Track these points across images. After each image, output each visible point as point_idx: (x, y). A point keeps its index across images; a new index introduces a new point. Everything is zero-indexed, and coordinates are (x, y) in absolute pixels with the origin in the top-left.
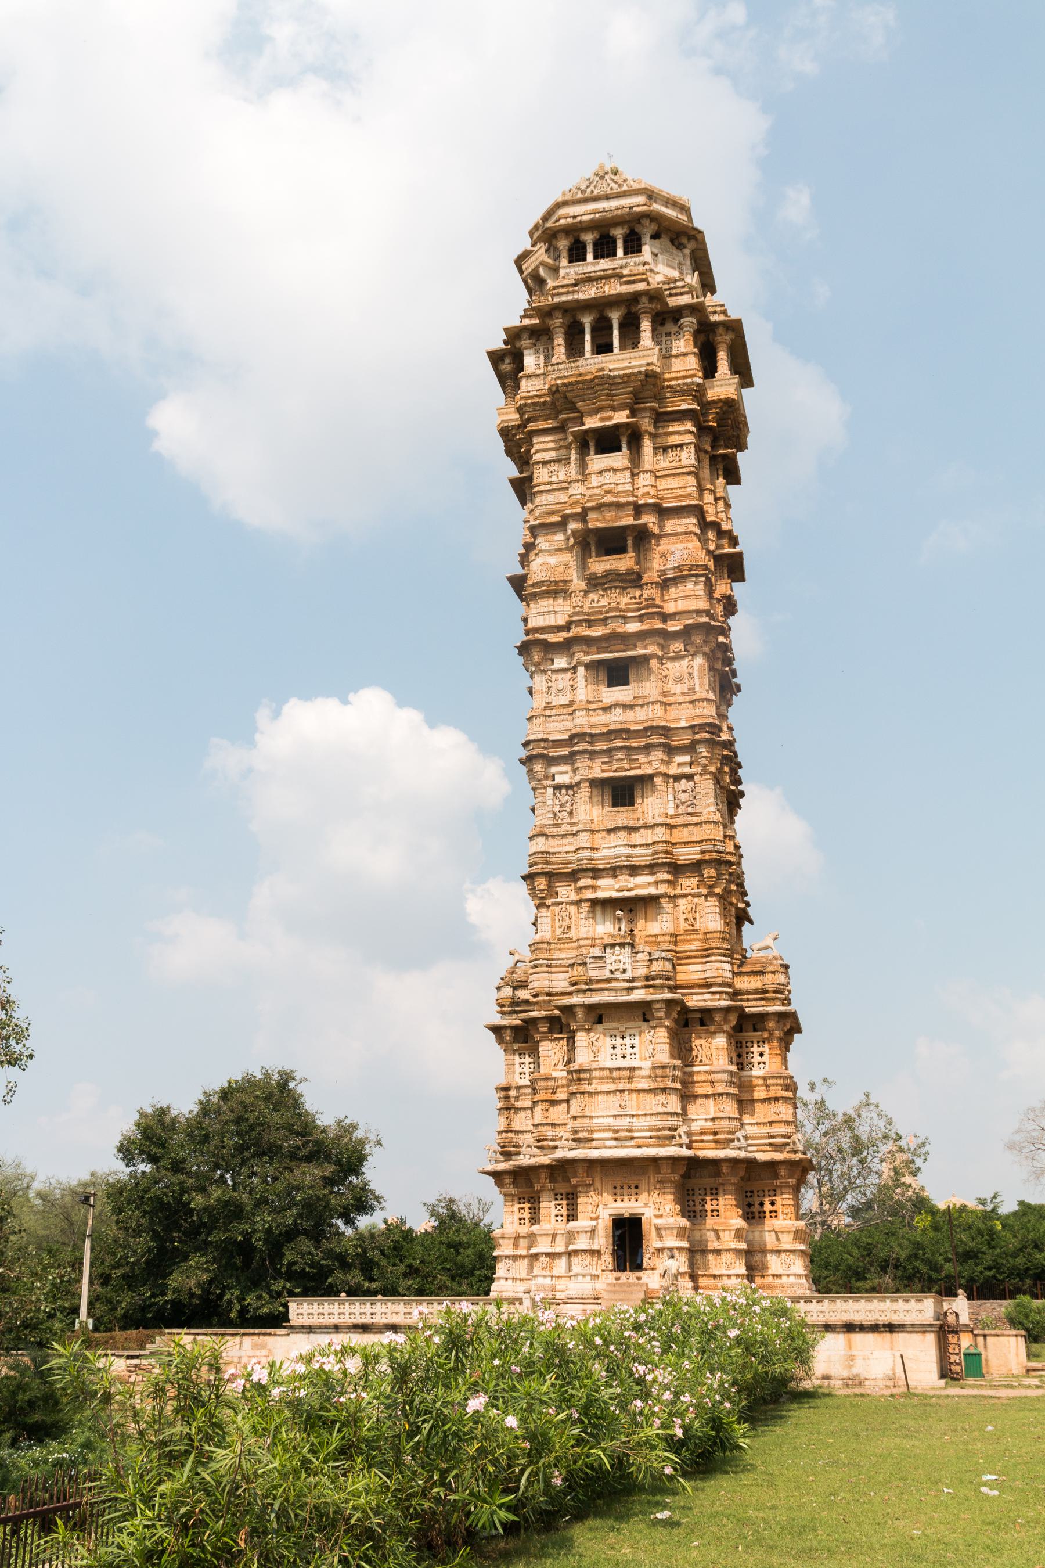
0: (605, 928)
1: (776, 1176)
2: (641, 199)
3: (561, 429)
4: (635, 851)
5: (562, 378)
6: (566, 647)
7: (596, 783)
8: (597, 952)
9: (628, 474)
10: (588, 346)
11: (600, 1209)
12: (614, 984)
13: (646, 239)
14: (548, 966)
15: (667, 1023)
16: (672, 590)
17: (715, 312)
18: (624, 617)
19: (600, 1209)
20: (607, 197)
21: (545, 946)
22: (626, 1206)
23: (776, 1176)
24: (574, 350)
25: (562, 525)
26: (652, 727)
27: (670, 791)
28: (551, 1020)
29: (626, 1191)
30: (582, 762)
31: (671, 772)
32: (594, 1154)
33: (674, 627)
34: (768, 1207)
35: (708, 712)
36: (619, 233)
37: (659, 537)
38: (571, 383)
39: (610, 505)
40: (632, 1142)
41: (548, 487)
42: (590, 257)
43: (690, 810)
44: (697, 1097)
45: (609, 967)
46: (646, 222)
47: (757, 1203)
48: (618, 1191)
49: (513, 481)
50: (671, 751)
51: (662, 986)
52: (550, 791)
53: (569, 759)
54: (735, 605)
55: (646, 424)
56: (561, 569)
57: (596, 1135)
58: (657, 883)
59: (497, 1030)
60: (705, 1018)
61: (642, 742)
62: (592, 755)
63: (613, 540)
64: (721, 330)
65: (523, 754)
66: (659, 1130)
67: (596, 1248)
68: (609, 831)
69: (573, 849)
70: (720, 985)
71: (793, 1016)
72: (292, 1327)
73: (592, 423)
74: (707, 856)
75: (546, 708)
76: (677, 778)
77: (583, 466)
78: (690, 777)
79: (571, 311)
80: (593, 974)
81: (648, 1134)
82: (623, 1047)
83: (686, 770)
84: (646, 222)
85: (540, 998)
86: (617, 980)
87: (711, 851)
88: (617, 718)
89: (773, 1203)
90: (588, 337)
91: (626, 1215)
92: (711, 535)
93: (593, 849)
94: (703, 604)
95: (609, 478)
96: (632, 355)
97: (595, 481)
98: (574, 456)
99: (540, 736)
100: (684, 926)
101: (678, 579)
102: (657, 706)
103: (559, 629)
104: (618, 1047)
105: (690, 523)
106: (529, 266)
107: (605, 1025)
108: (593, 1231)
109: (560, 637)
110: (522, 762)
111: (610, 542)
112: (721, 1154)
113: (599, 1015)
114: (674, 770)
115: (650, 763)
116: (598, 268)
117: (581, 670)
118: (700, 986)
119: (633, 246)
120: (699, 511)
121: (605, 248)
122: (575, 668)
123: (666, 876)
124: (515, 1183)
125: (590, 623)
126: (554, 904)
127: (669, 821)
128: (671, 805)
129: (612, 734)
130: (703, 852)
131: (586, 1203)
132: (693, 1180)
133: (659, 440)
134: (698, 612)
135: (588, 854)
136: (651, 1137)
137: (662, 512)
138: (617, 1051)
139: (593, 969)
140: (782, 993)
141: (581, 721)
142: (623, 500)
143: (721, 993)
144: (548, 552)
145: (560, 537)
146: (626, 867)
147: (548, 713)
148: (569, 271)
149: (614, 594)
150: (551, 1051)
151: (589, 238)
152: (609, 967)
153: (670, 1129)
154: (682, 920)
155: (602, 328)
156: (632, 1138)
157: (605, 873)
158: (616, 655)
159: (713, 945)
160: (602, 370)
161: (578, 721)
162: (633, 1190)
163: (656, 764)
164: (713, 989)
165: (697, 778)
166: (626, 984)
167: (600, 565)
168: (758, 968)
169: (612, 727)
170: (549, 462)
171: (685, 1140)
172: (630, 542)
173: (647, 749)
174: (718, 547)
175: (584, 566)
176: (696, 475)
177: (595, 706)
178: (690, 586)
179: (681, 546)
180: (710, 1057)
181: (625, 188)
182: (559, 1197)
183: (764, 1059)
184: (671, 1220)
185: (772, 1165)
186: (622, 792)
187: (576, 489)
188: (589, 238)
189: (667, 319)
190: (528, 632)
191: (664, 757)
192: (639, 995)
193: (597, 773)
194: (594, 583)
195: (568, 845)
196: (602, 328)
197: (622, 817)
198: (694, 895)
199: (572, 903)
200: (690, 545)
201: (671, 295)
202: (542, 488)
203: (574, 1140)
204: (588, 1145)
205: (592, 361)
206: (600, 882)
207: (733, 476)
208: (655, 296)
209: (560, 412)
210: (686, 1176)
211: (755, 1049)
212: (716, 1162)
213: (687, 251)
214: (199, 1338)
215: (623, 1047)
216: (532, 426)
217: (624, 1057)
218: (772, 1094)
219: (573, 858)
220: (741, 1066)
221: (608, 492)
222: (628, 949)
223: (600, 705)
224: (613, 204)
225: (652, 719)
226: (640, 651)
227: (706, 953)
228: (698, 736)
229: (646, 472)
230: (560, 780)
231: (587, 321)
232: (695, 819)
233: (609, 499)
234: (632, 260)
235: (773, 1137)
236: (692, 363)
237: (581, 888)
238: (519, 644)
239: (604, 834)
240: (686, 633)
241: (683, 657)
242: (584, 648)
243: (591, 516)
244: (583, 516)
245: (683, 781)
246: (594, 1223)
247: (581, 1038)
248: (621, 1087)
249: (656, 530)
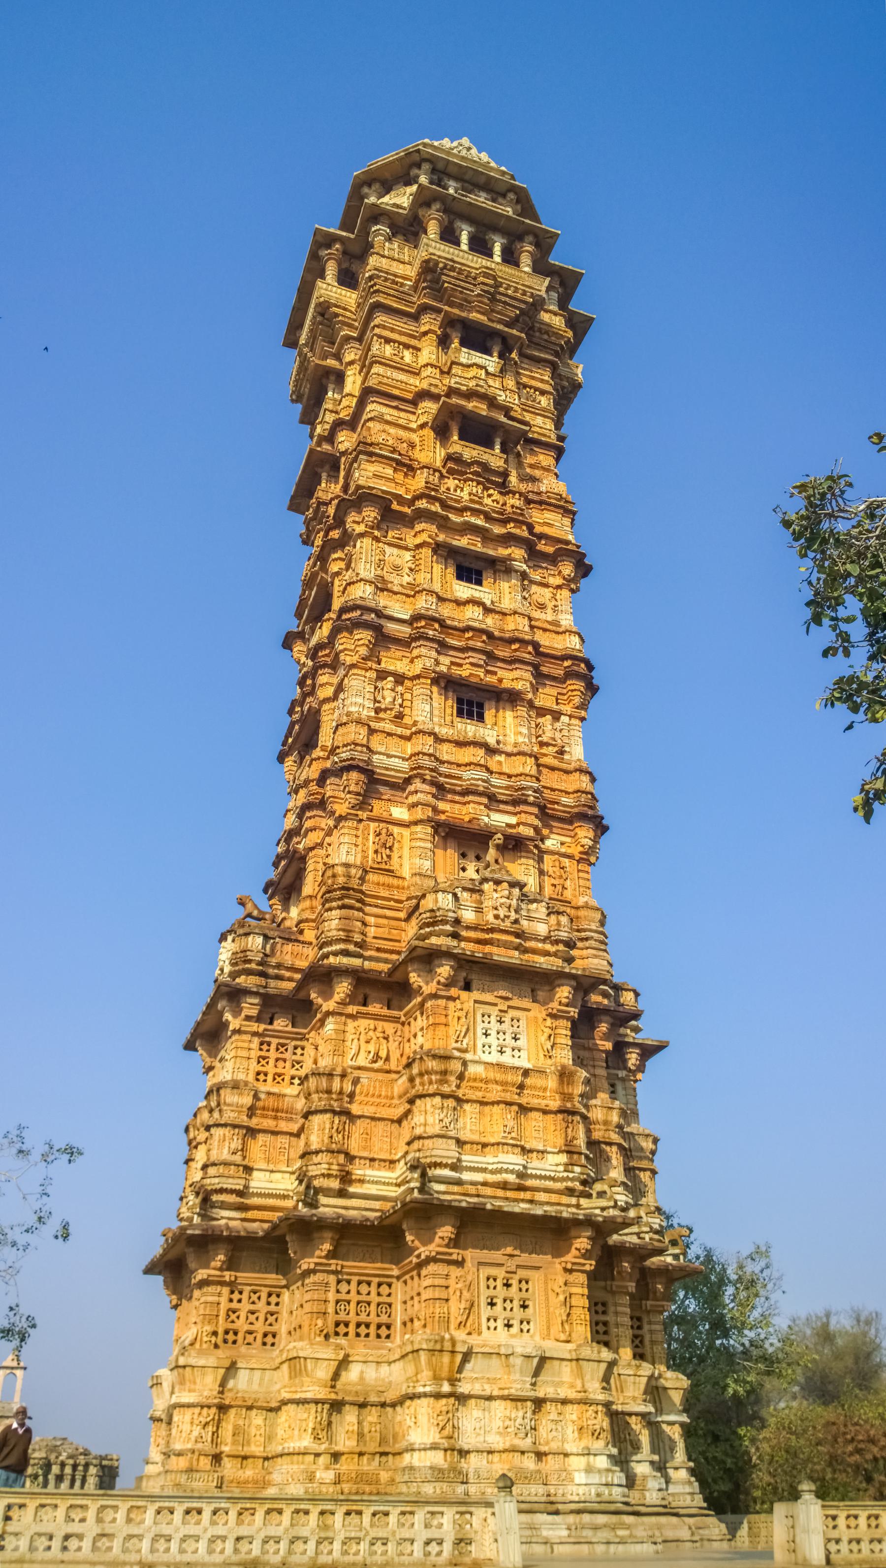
31: (537, 703)
76: (542, 712)
82: (501, 1036)
104: (493, 1033)
107: (476, 995)
117: (427, 552)
138: (492, 1039)
206: (442, 805)
215: (501, 1036)
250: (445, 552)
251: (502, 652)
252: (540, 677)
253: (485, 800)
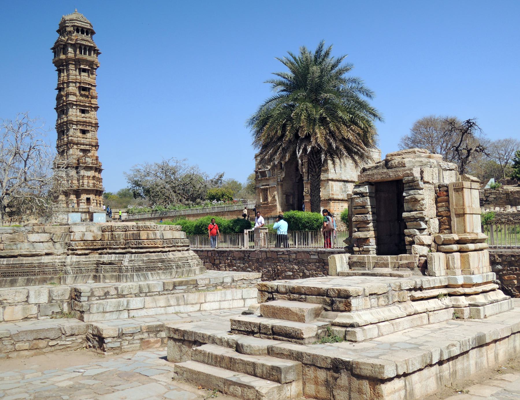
0: (81, 154)
6: (76, 105)
7: (80, 130)
22: (88, 196)
25: (75, 83)
30: (79, 126)
33: (93, 106)
50: (92, 127)
53: (77, 125)
62: (80, 125)
63: (84, 89)
73: (82, 67)
79: (81, 45)
88: (84, 119)
95: (85, 77)
97: (82, 77)
98: (78, 70)
109: (75, 103)
111: (84, 89)
115: (88, 128)
119: (87, 34)
121: (83, 33)
129: (83, 122)
141: (79, 119)
173: (89, 126)
175: (80, 92)
186: (84, 132)
192: (90, 165)
194: (81, 95)
195: (76, 139)
216: (70, 62)
244: (80, 83)
250: (80, 109)
251: (88, 124)
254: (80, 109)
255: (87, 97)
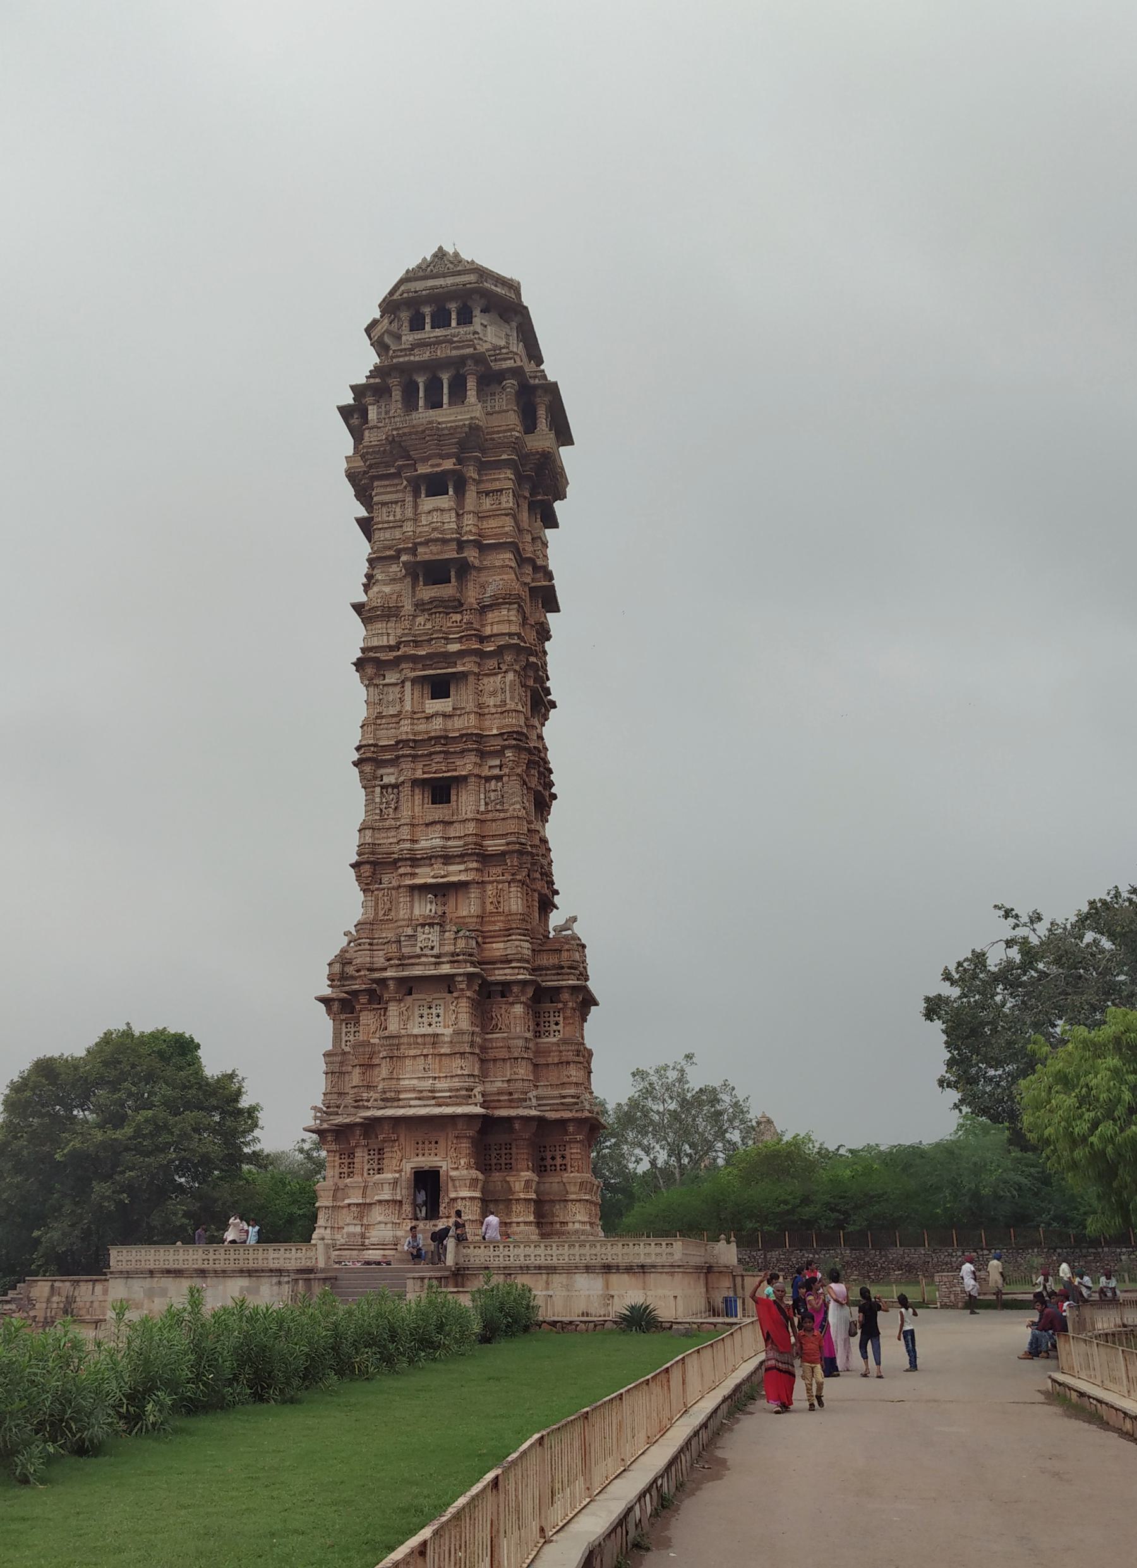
1: (566, 1133)
2: (472, 278)
3: (398, 475)
4: (450, 843)
5: (396, 429)
6: (396, 663)
7: (415, 783)
8: (409, 931)
9: (453, 514)
10: (421, 403)
11: (404, 1163)
12: (423, 959)
13: (477, 312)
14: (370, 944)
15: (468, 994)
16: (490, 615)
17: (535, 377)
18: (446, 639)
19: (404, 1163)
20: (444, 276)
21: (368, 926)
22: (426, 1161)
23: (566, 1133)
24: (410, 403)
26: (467, 734)
27: (482, 790)
28: (371, 992)
29: (427, 1145)
30: (406, 765)
32: (400, 1112)
34: (559, 1161)
35: (515, 722)
36: (453, 306)
37: (479, 569)
38: (405, 434)
39: (437, 540)
40: (433, 1102)
41: (386, 525)
42: (428, 327)
43: (498, 807)
44: (495, 1060)
45: (419, 945)
46: (476, 297)
47: (549, 1157)
48: (420, 1145)
49: (360, 521)
50: (483, 754)
51: (466, 961)
52: (378, 789)
54: (549, 632)
55: (471, 473)
56: (395, 596)
57: (402, 1096)
58: (466, 870)
59: (325, 1001)
60: (505, 988)
61: (459, 747)
64: (539, 392)
65: (356, 756)
66: (457, 1090)
67: (399, 1198)
68: (427, 825)
69: (395, 840)
70: (519, 961)
71: (585, 989)
72: (111, 1273)
73: (423, 469)
74: (511, 847)
75: (377, 718)
76: (488, 779)
77: (416, 506)
78: (499, 778)
79: (406, 372)
80: (406, 950)
81: (448, 1094)
83: (496, 772)
84: (476, 297)
85: (362, 973)
86: (426, 956)
87: (514, 843)
88: (437, 725)
89: (563, 1157)
90: (421, 394)
91: (426, 1168)
92: (528, 569)
93: (413, 841)
94: (514, 629)
95: (436, 517)
96: (459, 410)
98: (409, 499)
99: (371, 742)
100: (490, 908)
101: (494, 606)
102: (472, 716)
103: (391, 648)
104: (425, 1016)
105: (507, 557)
106: (376, 333)
107: (414, 996)
108: (396, 1182)
110: (355, 764)
111: (435, 572)
112: (513, 1113)
113: (408, 986)
114: (486, 772)
115: (466, 766)
116: (435, 334)
117: (408, 685)
118: (502, 962)
119: (465, 318)
120: (515, 548)
121: (442, 320)
122: (403, 682)
123: (475, 865)
124: (337, 1140)
125: (417, 644)
126: (377, 889)
127: (479, 817)
128: (483, 802)
130: (508, 844)
131: (392, 1159)
132: (490, 1138)
133: (482, 486)
134: (510, 635)
135: (408, 845)
136: (450, 1097)
137: (482, 548)
139: (406, 946)
140: (575, 969)
141: (405, 729)
142: (448, 536)
143: (519, 968)
144: (385, 583)
145: (394, 568)
146: (440, 856)
147: (379, 721)
148: (409, 338)
149: (439, 618)
150: (368, 1019)
151: (427, 310)
152: (419, 945)
153: (467, 1090)
154: (488, 904)
155: (434, 388)
156: (434, 1098)
157: (422, 862)
158: (439, 671)
159: (514, 926)
160: (431, 422)
161: (404, 729)
162: (433, 1145)
163: (469, 767)
164: (513, 965)
165: (505, 779)
166: (433, 959)
167: (428, 593)
168: (557, 946)
169: (433, 734)
170: (387, 503)
171: (480, 1099)
172: (453, 573)
174: (533, 580)
176: (514, 517)
177: (419, 715)
178: (505, 612)
179: (497, 578)
180: (508, 1027)
181: (459, 268)
182: (372, 1152)
183: (558, 1028)
184: (465, 1172)
185: (562, 1123)
186: (440, 791)
187: (408, 527)
188: (427, 310)
189: (490, 380)
190: (363, 650)
191: (478, 761)
192: (446, 969)
193: (419, 774)
196: (434, 388)
197: (439, 812)
198: (498, 882)
199: (393, 888)
200: (506, 577)
201: (496, 360)
202: (380, 526)
203: (382, 1100)
204: (396, 1104)
205: (424, 415)
206: (417, 871)
207: (551, 521)
208: (479, 359)
209: (397, 460)
210: (482, 1132)
211: (552, 1019)
212: (509, 1119)
213: (514, 324)
214: (57, 1284)
217: (430, 1025)
218: (564, 1059)
219: (396, 848)
220: (537, 1034)
221: (434, 529)
222: (437, 928)
223: (423, 715)
224: (450, 281)
225: (468, 728)
226: (460, 669)
227: (508, 932)
228: (506, 743)
229: (470, 513)
230: (386, 780)
231: (421, 381)
232: (502, 815)
233: (436, 535)
234: (462, 330)
235: (564, 1097)
236: (513, 419)
237: (401, 875)
238: (355, 660)
239: (423, 828)
240: (500, 651)
241: (496, 674)
242: (411, 665)
243: (420, 550)
245: (493, 782)
246: (397, 1175)
247: (393, 1009)
248: (425, 1052)
249: (477, 563)
252: (483, 754)
253: (440, 860)
254: (414, 681)
255: (457, 605)
